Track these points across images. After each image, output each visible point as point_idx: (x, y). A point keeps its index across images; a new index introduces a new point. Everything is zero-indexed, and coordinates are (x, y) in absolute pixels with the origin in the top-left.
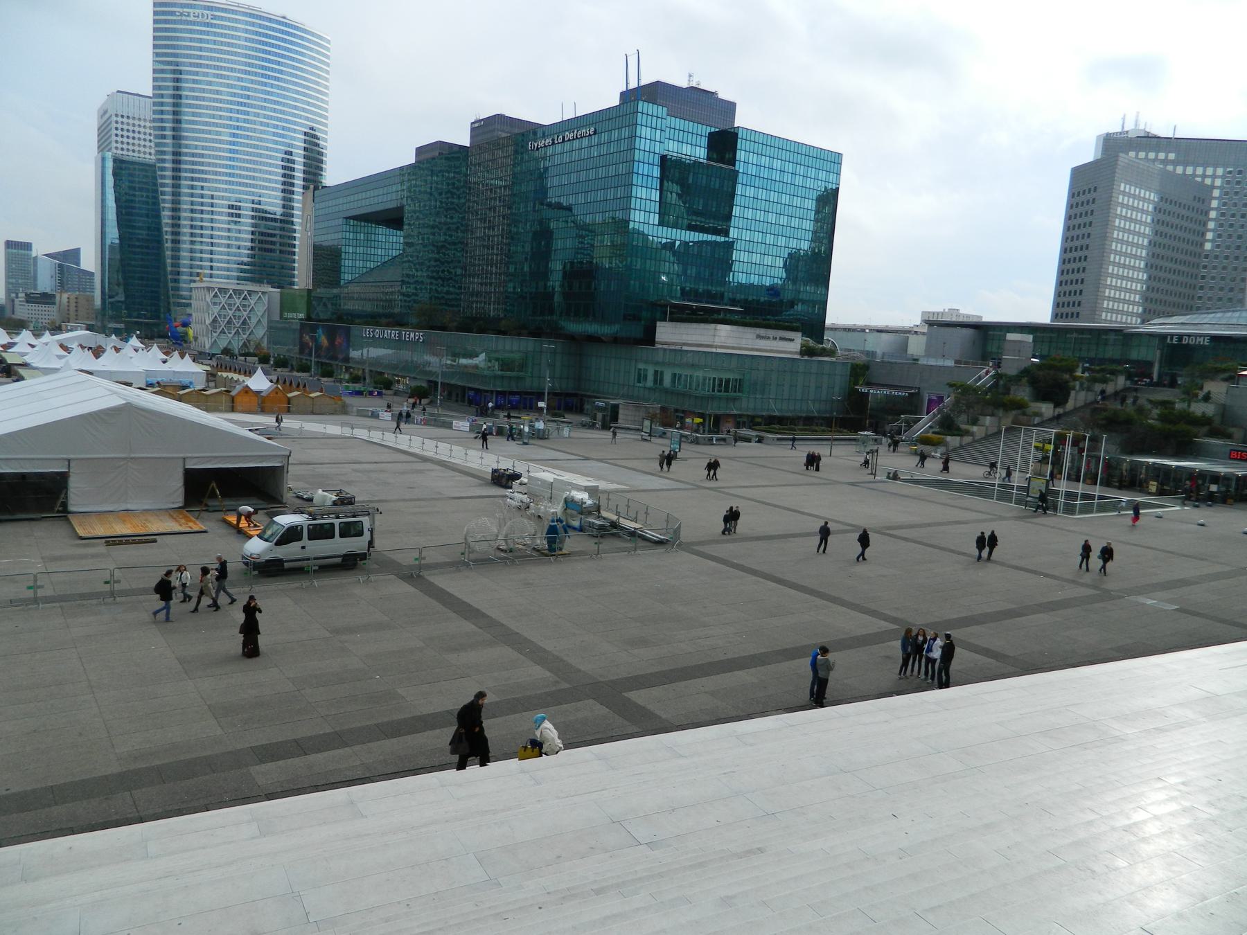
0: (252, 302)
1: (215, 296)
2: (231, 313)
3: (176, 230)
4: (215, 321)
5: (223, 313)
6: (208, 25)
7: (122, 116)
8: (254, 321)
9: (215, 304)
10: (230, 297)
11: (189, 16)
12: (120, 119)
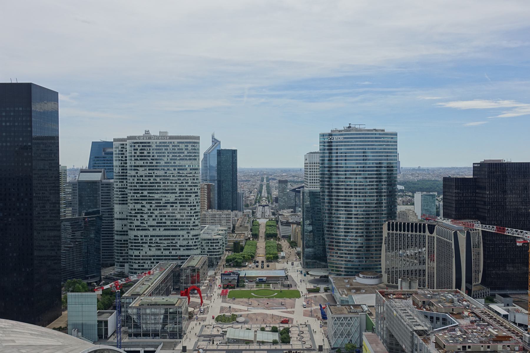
0: (352, 323)
1: (336, 320)
2: (342, 328)
3: (331, 226)
4: (335, 332)
5: (339, 328)
6: (342, 142)
7: (312, 163)
8: (353, 330)
9: (335, 324)
10: (342, 320)
11: (333, 139)
12: (311, 165)
